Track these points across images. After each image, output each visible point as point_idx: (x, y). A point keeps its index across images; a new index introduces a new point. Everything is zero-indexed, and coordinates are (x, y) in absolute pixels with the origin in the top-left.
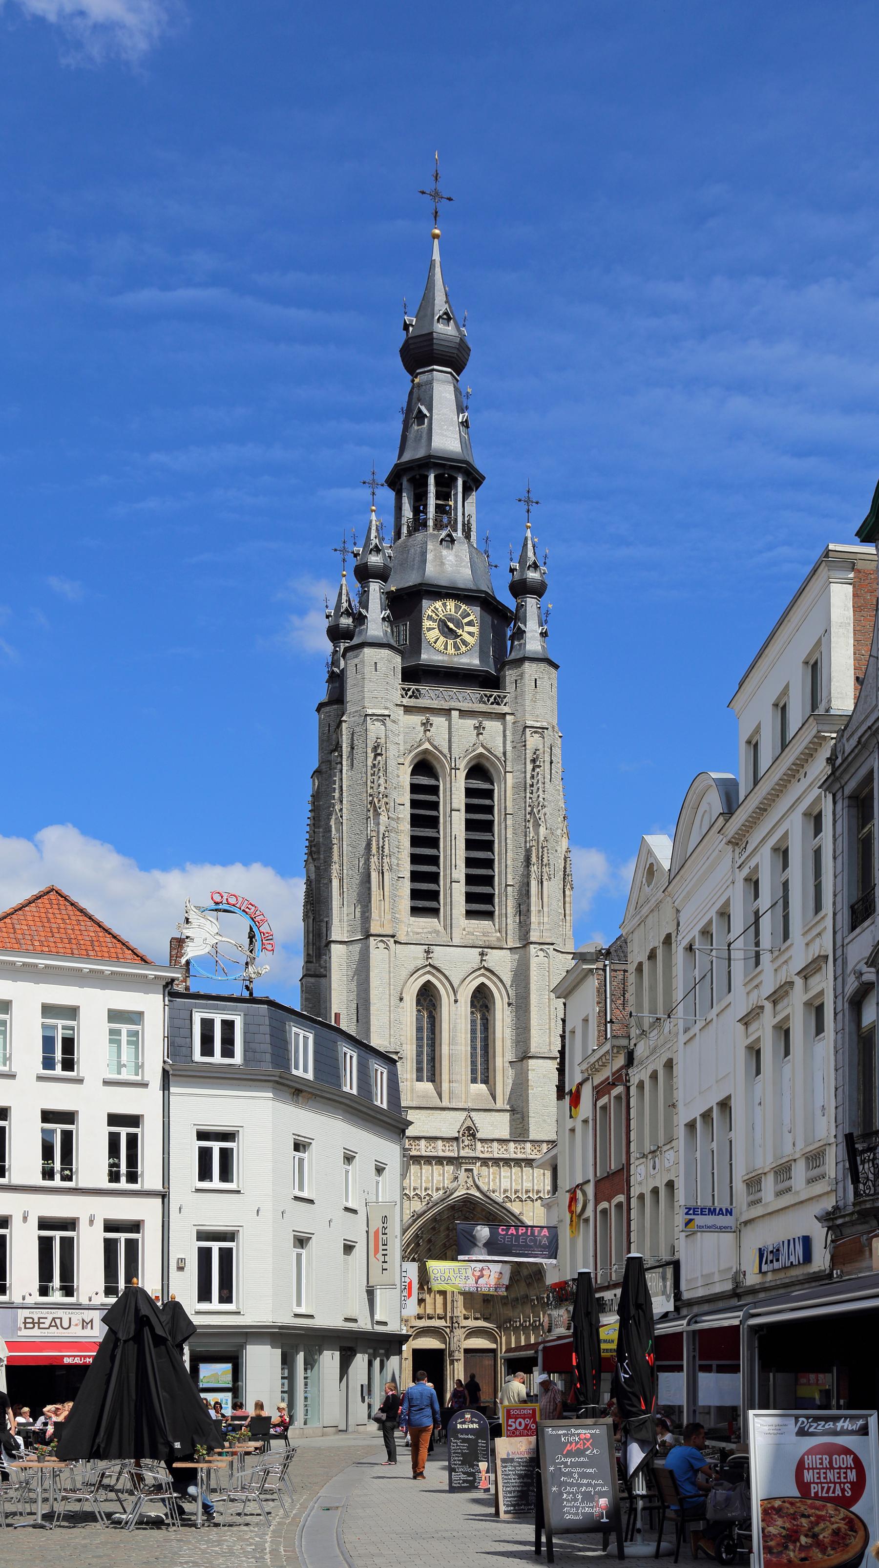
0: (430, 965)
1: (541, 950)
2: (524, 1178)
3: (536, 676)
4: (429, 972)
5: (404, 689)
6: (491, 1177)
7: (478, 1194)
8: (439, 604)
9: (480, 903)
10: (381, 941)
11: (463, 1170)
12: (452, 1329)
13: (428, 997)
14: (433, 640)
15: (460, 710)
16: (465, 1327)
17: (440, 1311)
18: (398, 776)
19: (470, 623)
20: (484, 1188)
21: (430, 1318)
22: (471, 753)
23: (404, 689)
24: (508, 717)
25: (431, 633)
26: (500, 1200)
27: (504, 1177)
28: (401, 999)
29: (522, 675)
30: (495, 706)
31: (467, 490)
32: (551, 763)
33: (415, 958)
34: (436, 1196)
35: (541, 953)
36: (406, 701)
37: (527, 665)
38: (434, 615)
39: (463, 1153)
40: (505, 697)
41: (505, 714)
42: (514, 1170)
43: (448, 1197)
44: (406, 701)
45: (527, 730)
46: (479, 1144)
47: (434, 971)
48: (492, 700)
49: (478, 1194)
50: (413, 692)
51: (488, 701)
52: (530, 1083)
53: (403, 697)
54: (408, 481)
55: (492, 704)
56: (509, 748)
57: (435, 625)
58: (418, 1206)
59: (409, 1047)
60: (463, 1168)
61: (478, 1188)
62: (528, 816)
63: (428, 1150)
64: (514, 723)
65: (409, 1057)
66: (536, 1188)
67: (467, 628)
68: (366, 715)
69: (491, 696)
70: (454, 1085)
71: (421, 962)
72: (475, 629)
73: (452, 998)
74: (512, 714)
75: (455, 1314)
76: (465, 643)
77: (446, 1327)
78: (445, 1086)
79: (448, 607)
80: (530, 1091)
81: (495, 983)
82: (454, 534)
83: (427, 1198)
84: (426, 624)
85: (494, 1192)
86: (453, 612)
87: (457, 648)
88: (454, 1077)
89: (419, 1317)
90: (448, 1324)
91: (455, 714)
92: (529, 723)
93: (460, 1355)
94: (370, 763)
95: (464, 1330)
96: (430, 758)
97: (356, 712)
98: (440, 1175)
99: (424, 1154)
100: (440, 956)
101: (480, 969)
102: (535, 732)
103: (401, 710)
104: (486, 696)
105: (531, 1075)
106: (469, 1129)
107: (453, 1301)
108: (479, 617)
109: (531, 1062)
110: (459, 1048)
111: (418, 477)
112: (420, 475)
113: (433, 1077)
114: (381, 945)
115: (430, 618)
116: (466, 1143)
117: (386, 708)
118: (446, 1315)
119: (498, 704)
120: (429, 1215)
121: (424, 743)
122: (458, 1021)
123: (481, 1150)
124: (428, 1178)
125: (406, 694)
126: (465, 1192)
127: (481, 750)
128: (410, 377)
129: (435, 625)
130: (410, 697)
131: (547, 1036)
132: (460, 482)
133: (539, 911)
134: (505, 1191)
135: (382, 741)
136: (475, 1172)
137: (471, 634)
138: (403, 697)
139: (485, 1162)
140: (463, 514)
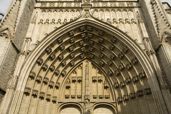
2: (117, 15)
11: (84, 10)
16: (93, 103)
17: (79, 93)
27: (107, 15)
34: (68, 21)
39: (83, 4)
42: (111, 13)
58: (59, 26)
60: (84, 10)
89: (67, 97)
90: (83, 101)
95: (92, 104)
107: (86, 87)
118: (82, 96)
124: (66, 17)
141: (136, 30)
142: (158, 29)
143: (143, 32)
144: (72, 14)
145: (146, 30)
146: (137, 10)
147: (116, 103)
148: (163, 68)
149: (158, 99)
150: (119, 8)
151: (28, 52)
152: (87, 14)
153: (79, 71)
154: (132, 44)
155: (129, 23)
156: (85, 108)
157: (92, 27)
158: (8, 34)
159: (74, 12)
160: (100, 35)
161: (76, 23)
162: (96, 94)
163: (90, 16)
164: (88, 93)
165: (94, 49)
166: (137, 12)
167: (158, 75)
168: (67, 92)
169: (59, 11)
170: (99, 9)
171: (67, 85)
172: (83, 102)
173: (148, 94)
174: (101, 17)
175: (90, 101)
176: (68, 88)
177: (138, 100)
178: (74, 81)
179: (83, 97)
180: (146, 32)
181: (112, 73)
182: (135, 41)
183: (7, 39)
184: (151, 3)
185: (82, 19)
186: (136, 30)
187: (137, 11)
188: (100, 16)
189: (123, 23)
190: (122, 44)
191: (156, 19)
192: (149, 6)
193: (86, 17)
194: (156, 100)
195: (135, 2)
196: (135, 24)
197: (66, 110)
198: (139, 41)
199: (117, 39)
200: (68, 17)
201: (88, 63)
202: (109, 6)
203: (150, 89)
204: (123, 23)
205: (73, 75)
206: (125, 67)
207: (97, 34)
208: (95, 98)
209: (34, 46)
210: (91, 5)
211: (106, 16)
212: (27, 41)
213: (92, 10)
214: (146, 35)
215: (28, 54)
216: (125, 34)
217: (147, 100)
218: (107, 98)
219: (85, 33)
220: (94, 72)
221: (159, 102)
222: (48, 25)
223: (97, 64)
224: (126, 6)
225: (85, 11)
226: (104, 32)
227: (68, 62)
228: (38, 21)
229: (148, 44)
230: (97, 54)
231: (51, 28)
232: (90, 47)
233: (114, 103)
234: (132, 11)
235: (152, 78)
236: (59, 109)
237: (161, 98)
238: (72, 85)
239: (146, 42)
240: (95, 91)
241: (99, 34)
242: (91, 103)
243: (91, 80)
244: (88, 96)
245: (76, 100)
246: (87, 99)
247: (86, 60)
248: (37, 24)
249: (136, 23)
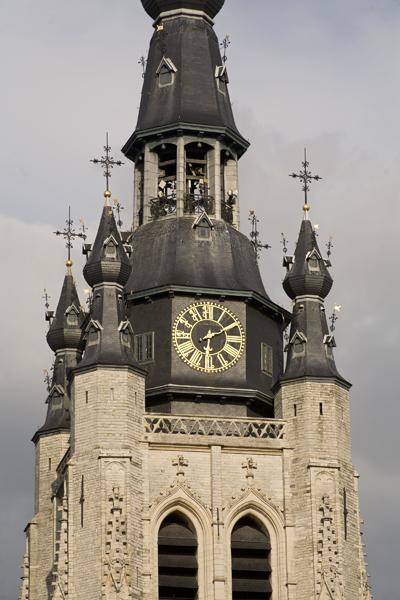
3: (321, 400)
5: (148, 420)
8: (192, 310)
14: (184, 355)
15: (223, 447)
18: (142, 536)
19: (234, 332)
22: (237, 502)
23: (148, 420)
25: (184, 348)
29: (301, 399)
30: (268, 439)
31: (224, 159)
32: (346, 513)
38: (186, 323)
40: (281, 427)
41: (282, 449)
44: (152, 437)
48: (264, 431)
50: (161, 424)
51: (259, 432)
53: (147, 431)
54: (151, 151)
55: (265, 436)
56: (289, 495)
57: (188, 336)
62: (318, 587)
64: (295, 460)
67: (229, 338)
69: (263, 426)
72: (240, 339)
76: (227, 356)
79: (205, 313)
82: (209, 218)
84: (177, 334)
86: (211, 318)
87: (217, 363)
92: (314, 461)
94: (104, 521)
97: (87, 453)
102: (323, 472)
103: (144, 450)
104: (256, 425)
108: (245, 324)
111: (163, 147)
112: (165, 144)
115: (181, 327)
117: (127, 447)
119: (272, 436)
121: (175, 491)
125: (152, 427)
128: (152, 21)
129: (188, 336)
130: (157, 431)
132: (217, 153)
137: (235, 345)
138: (147, 431)
140: (223, 190)
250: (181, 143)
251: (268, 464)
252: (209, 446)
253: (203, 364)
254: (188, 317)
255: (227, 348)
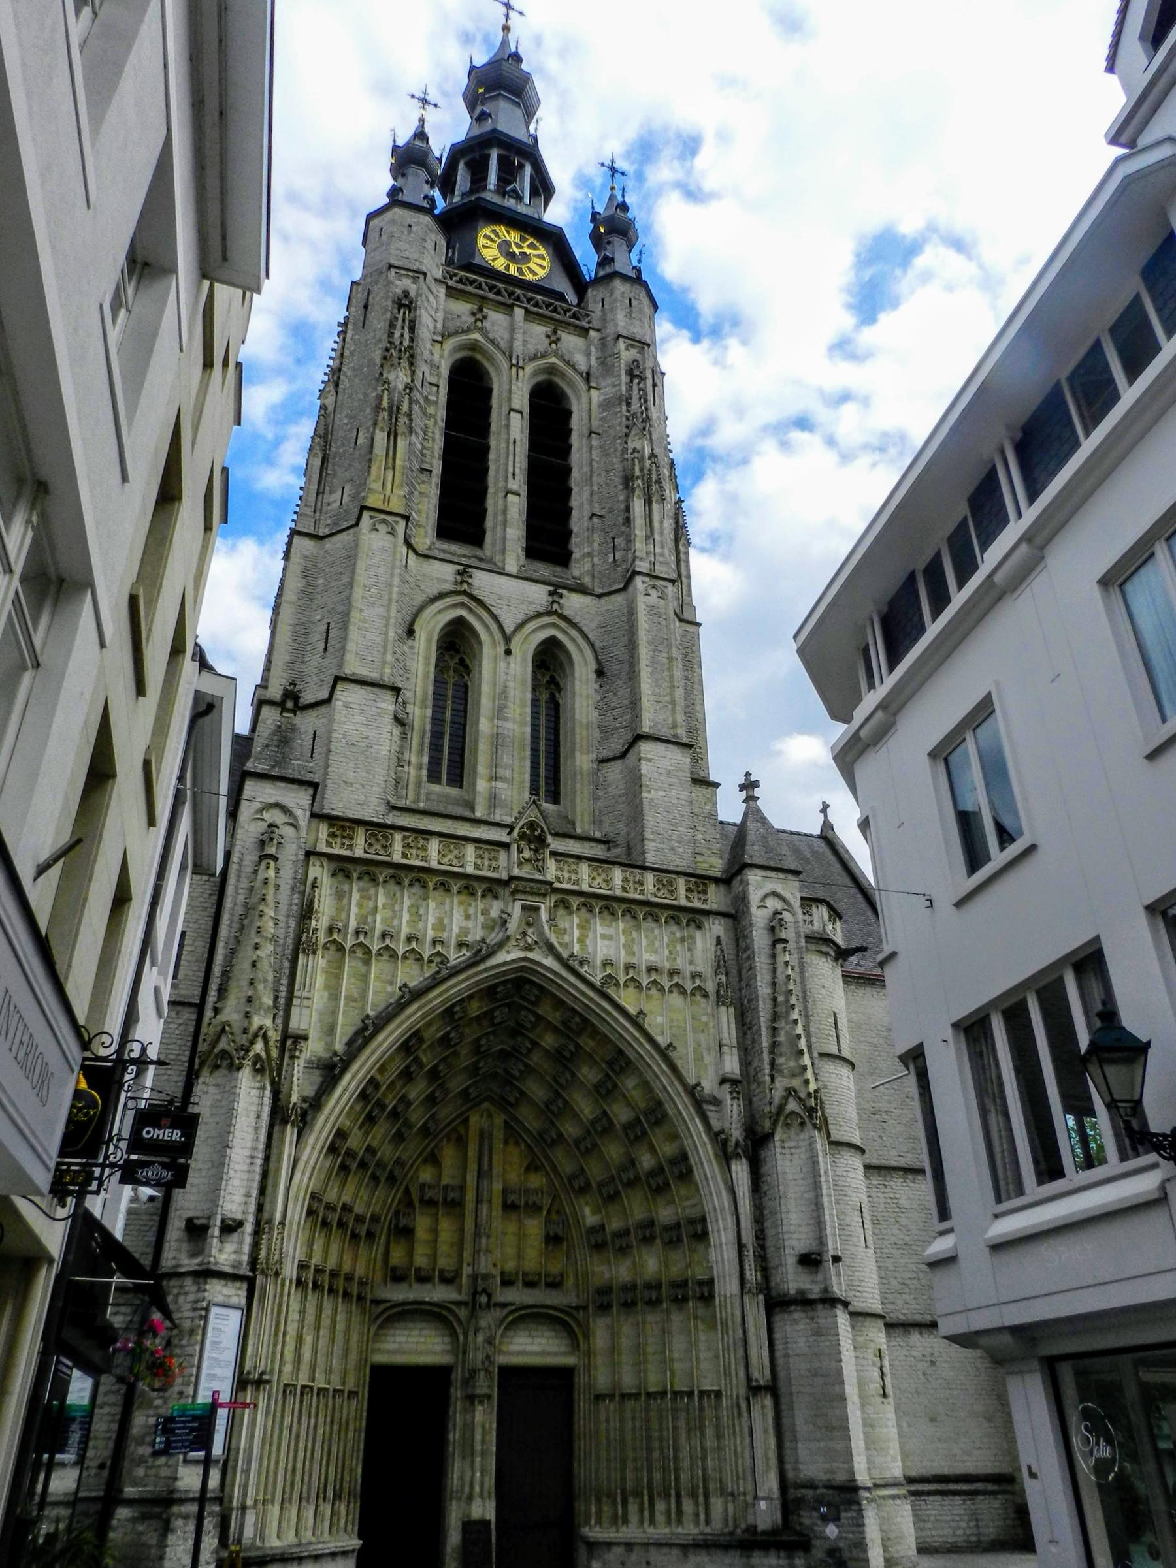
0: (465, 593)
1: (654, 587)
4: (463, 605)
6: (576, 933)
7: (549, 962)
8: (502, 229)
9: (549, 540)
10: (384, 521)
11: (518, 904)
12: (473, 1305)
13: (456, 645)
16: (503, 1305)
17: (445, 1262)
19: (541, 257)
20: (565, 955)
21: (423, 1278)
24: (592, 333)
26: (598, 983)
27: (604, 937)
28: (410, 632)
33: (440, 580)
34: (455, 957)
35: (653, 592)
36: (450, 283)
37: (617, 283)
39: (516, 872)
40: (588, 315)
43: (484, 959)
45: (621, 340)
46: (552, 867)
47: (473, 605)
49: (549, 962)
52: (645, 781)
54: (467, 164)
56: (593, 362)
59: (417, 711)
60: (518, 904)
61: (551, 949)
63: (446, 860)
65: (417, 725)
66: (667, 965)
68: (391, 266)
70: (499, 784)
71: (449, 587)
73: (501, 649)
74: (599, 330)
75: (483, 1271)
77: (458, 1304)
78: (482, 785)
80: (644, 795)
81: (573, 640)
83: (438, 959)
85: (581, 963)
88: (501, 772)
89: (397, 1276)
91: (519, 312)
93: (486, 1385)
95: (498, 1313)
96: (479, 357)
98: (467, 917)
99: (434, 864)
100: (482, 582)
101: (549, 613)
102: (632, 346)
103: (443, 290)
104: (562, 308)
105: (645, 768)
106: (532, 825)
109: (645, 748)
110: (509, 725)
113: (457, 777)
114: (383, 529)
115: (486, 237)
116: (527, 854)
118: (458, 1273)
119: (578, 319)
120: (436, 999)
122: (511, 684)
123: (552, 870)
126: (521, 954)
127: (554, 360)
131: (668, 713)
133: (647, 538)
134: (606, 963)
135: (412, 294)
136: (544, 915)
137: (543, 267)
139: (565, 899)
141: (703, 1031)
142: (772, 1064)
143: (725, 1049)
144: (466, 911)
145: (735, 1044)
146: (717, 928)
147: (585, 1308)
148: (762, 1214)
149: (730, 1323)
150: (652, 910)
151: (305, 1106)
152: (530, 931)
153: (449, 1155)
154: (683, 1105)
155: (682, 991)
156: (476, 1331)
157: (541, 988)
158: (263, 1054)
159: (473, 894)
160: (570, 1029)
161: (486, 970)
162: (510, 1266)
163: (541, 944)
164: (484, 1265)
165: (529, 1070)
166: (719, 942)
167: (744, 1241)
168: (397, 1256)
169: (411, 885)
170: (575, 902)
171: (403, 1222)
172: (465, 1304)
173: (702, 1298)
174: (581, 940)
175: (493, 1301)
176: (406, 1233)
177: (668, 1312)
178: (431, 1203)
179: (464, 1280)
180: (735, 1051)
181: (588, 1184)
182: (692, 1091)
183: (259, 1078)
184: (772, 929)
185: (508, 952)
186: (703, 1031)
187: (718, 938)
188: (576, 933)
189: (661, 989)
190: (646, 1086)
191: (775, 1017)
192: (760, 938)
193: (528, 948)
194: (724, 1324)
195: (717, 881)
196: (703, 1000)
197: (392, 1332)
198: (709, 1085)
199: (629, 1062)
200: (446, 921)
201: (490, 1116)
202: (619, 893)
203: (711, 1282)
204: (661, 989)
205: (426, 1175)
206: (640, 1178)
207: (555, 1017)
208: (507, 1282)
209: (318, 1072)
210: (551, 883)
211: (602, 943)
212: (297, 1054)
213: (551, 900)
214: (732, 1065)
215: (304, 1114)
216: (664, 1053)
217: (696, 1318)
218: (555, 1284)
219: (508, 1005)
220: (508, 1168)
221: (731, 1333)
222: (367, 962)
223: (527, 1130)
224: (683, 902)
225: (524, 908)
226: (585, 1020)
227: (418, 1117)
228: (322, 938)
229: (735, 1107)
230: (537, 1091)
231: (381, 984)
232: (513, 1060)
233: (577, 1308)
234: (699, 927)
235: (724, 1247)
236: (373, 1330)
237: (739, 1320)
238: (422, 1224)
239: (729, 1102)
240: (511, 1251)
241: (564, 1023)
242: (496, 1305)
243: (497, 1201)
244: (485, 1277)
245: (438, 1293)
246: (484, 1291)
247: (486, 1105)
248: (320, 952)
249: (706, 996)
250: (494, 154)
251: (570, 341)
252: (511, 306)
253: (507, 268)
254: (494, 232)
255: (531, 265)
